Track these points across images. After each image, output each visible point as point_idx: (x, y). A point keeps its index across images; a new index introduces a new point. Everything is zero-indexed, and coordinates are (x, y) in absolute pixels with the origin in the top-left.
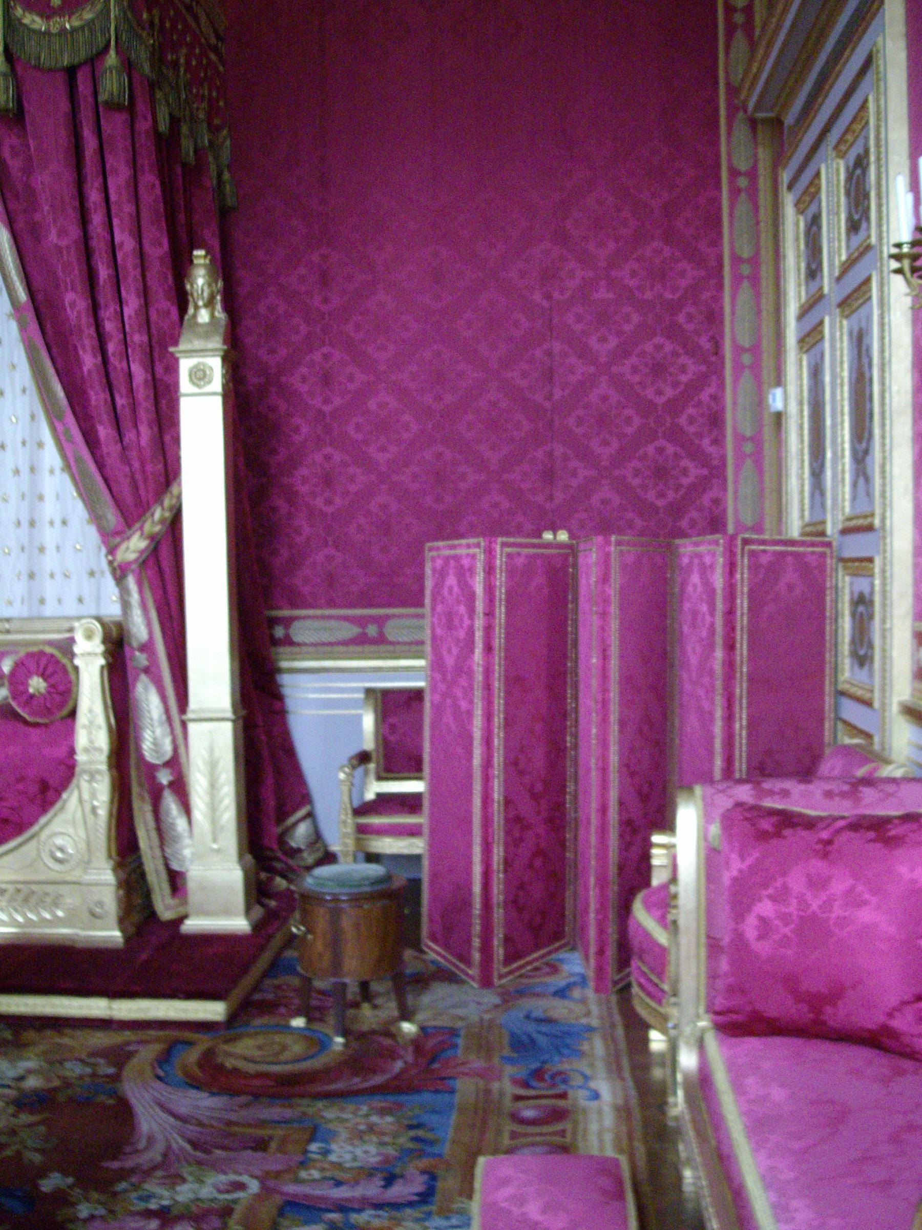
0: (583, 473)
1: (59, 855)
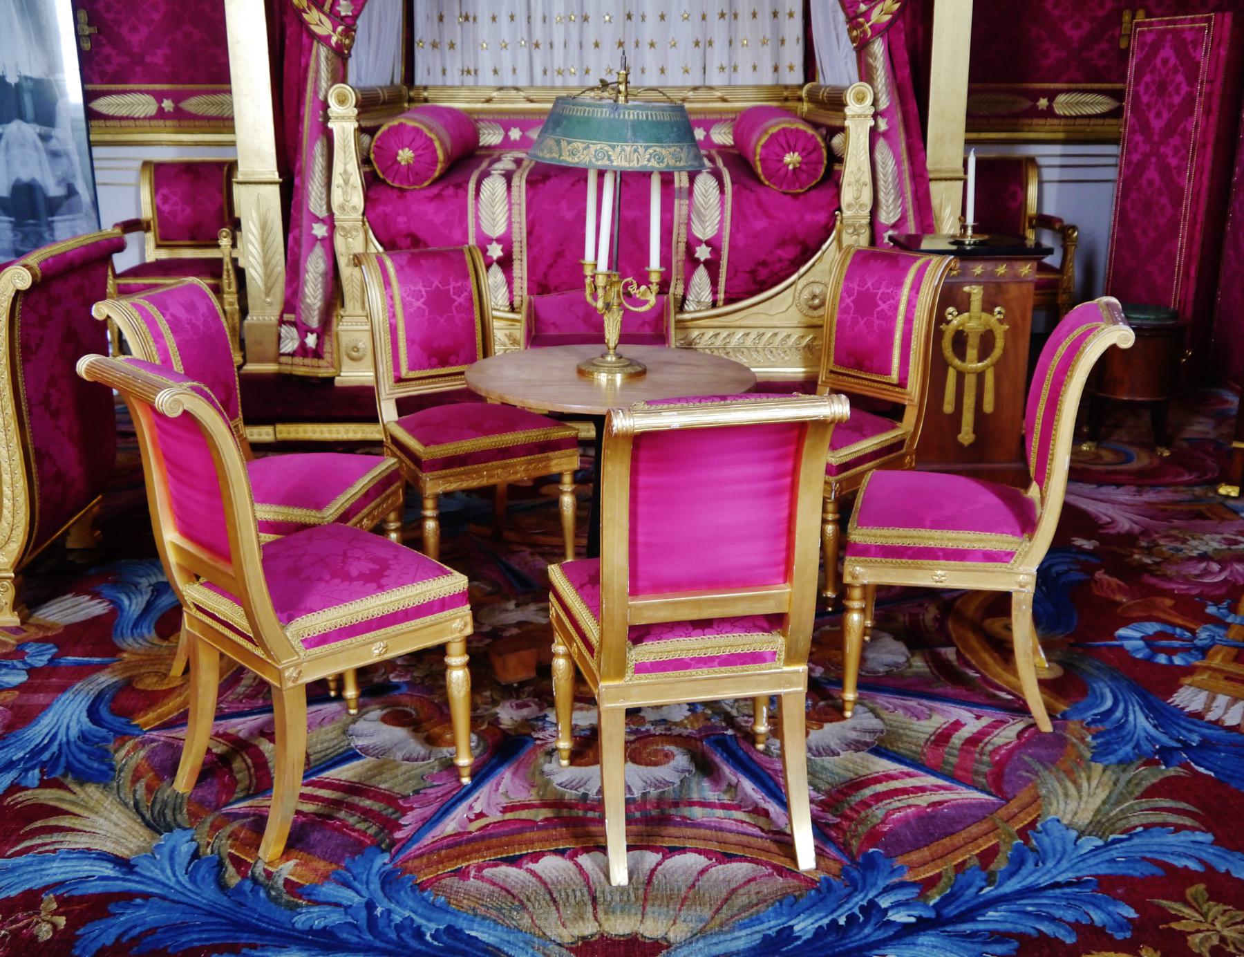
1: (817, 301)
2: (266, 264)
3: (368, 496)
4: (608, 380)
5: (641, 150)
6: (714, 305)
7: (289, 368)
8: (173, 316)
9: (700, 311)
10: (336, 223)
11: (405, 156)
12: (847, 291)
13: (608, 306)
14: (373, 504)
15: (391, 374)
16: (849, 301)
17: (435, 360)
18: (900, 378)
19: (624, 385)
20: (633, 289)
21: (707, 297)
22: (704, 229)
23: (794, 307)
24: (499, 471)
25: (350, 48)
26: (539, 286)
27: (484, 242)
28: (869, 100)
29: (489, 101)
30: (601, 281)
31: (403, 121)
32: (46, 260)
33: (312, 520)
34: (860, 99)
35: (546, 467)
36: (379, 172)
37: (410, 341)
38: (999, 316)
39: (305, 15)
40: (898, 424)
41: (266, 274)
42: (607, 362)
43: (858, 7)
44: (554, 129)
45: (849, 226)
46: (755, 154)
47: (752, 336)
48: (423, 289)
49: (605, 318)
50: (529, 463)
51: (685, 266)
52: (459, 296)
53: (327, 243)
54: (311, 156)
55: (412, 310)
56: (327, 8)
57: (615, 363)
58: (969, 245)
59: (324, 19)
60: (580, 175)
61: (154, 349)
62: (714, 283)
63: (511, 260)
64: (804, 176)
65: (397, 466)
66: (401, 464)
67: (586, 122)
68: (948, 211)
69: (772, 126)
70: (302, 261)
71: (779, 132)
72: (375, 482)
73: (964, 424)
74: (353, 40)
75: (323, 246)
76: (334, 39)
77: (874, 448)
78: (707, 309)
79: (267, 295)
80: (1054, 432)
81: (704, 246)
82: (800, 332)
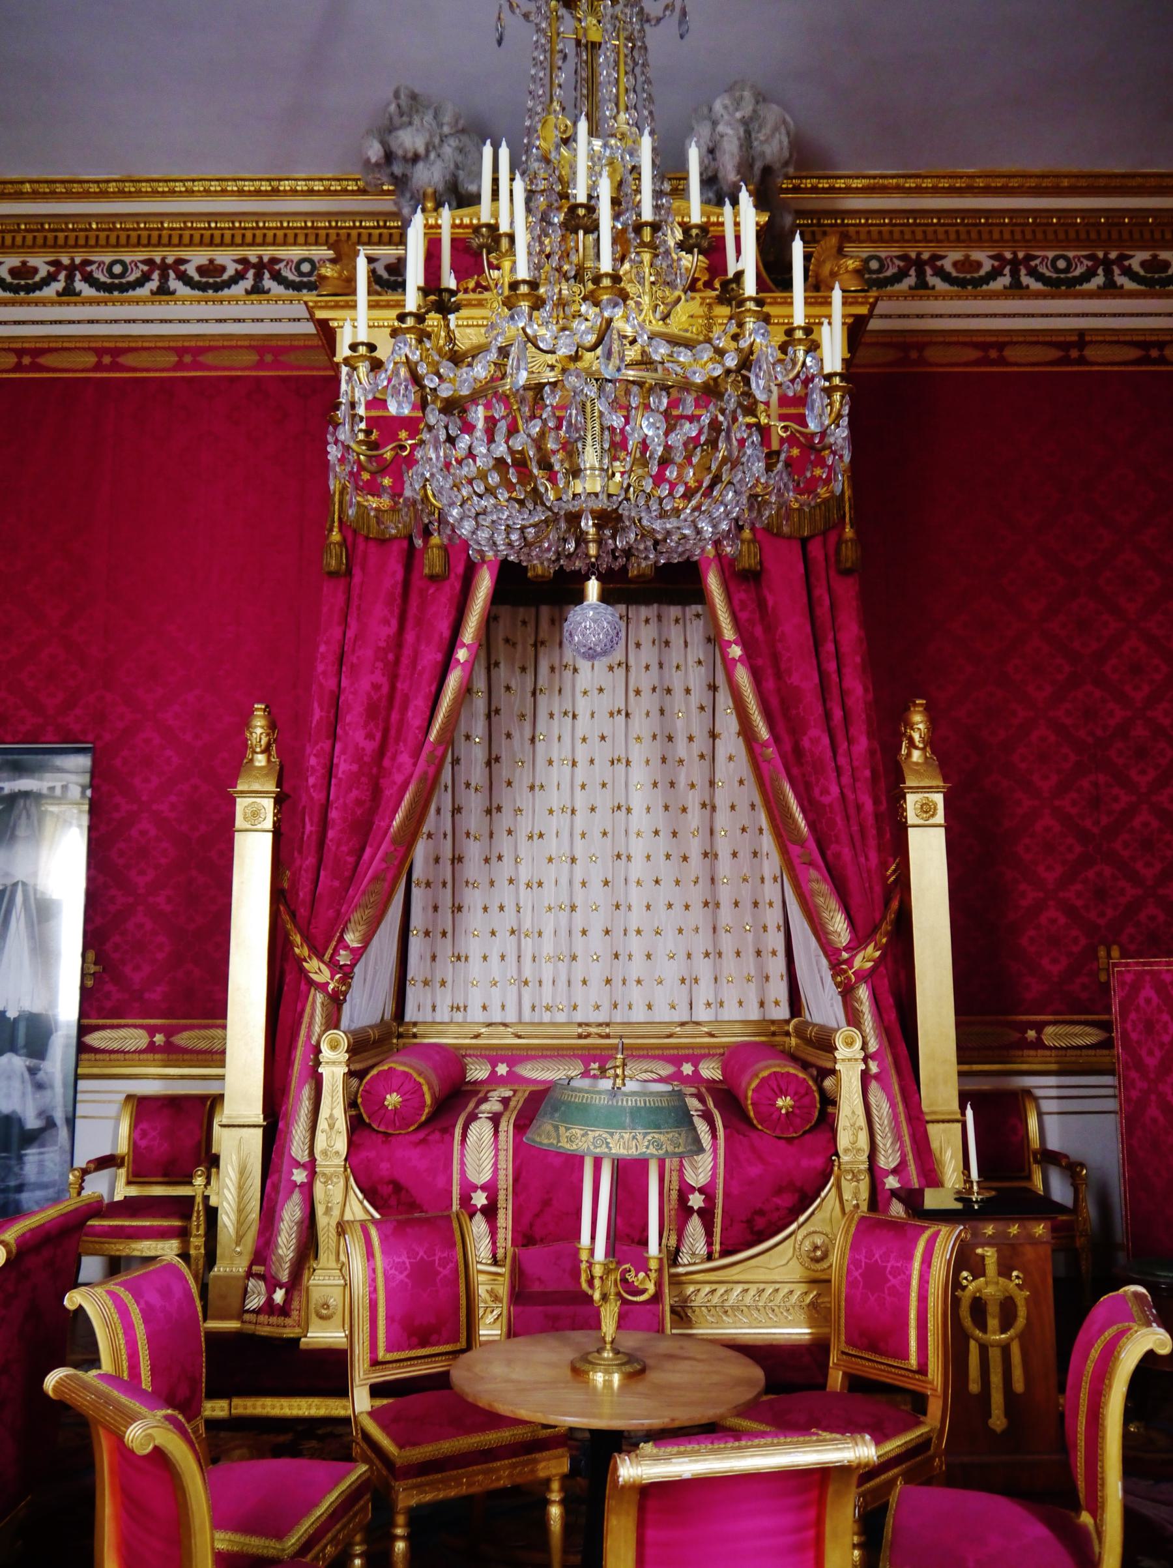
1: (819, 1253)
2: (240, 1211)
3: (335, 1515)
4: (605, 1381)
5: (639, 1137)
6: (710, 1257)
7: (252, 1327)
8: (147, 1303)
9: (694, 1264)
10: (318, 1170)
11: (393, 1100)
12: (854, 1263)
13: (605, 1297)
14: (338, 1526)
15: (367, 1356)
16: (856, 1274)
17: (415, 1340)
18: (919, 1364)
19: (622, 1386)
20: (630, 1277)
21: (701, 1248)
22: (697, 1176)
23: (794, 1262)
24: (480, 1477)
25: (345, 994)
26: (524, 1237)
27: (468, 1188)
28: (858, 1044)
29: (477, 1036)
30: (598, 1271)
31: (393, 1065)
32: (23, 1235)
33: (272, 1552)
34: (849, 1043)
35: (533, 1471)
36: (365, 1116)
37: (389, 1318)
38: (1017, 1281)
39: (305, 964)
40: (922, 1418)
41: (238, 1222)
42: (604, 1359)
43: (840, 955)
44: (552, 1114)
45: (847, 1171)
46: (746, 1098)
47: (752, 1292)
48: (407, 1261)
49: (602, 1309)
50: (514, 1466)
51: (677, 1215)
52: (444, 1268)
53: (306, 1189)
54: (298, 1099)
55: (394, 1285)
56: (327, 957)
57: (612, 1360)
58: (977, 1202)
59: (323, 967)
60: (574, 1162)
61: (122, 1342)
62: (709, 1234)
63: (497, 1209)
64: (798, 1120)
65: (368, 1474)
66: (372, 1472)
67: (584, 1108)
68: (949, 1154)
69: (762, 1070)
70: (278, 1208)
71: (770, 1075)
72: (343, 1497)
73: (994, 1406)
74: (349, 986)
75: (301, 1193)
76: (331, 987)
77: (898, 1451)
78: (702, 1262)
79: (238, 1244)
80: (1100, 1452)
81: (697, 1193)
82: (802, 1288)
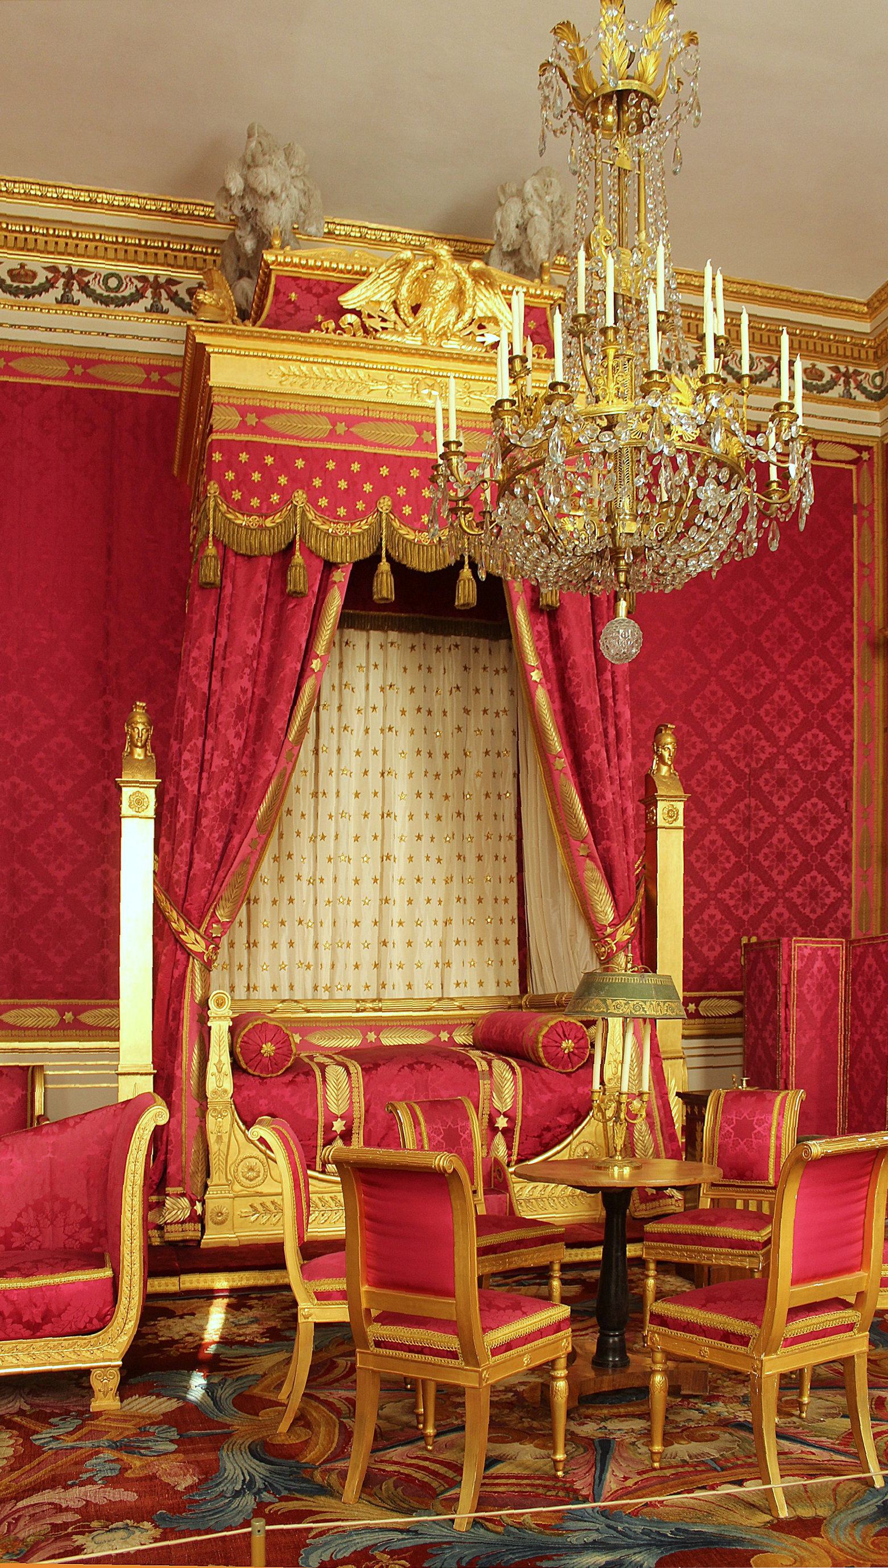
0: (767, 894)
63: (352, 1134)
